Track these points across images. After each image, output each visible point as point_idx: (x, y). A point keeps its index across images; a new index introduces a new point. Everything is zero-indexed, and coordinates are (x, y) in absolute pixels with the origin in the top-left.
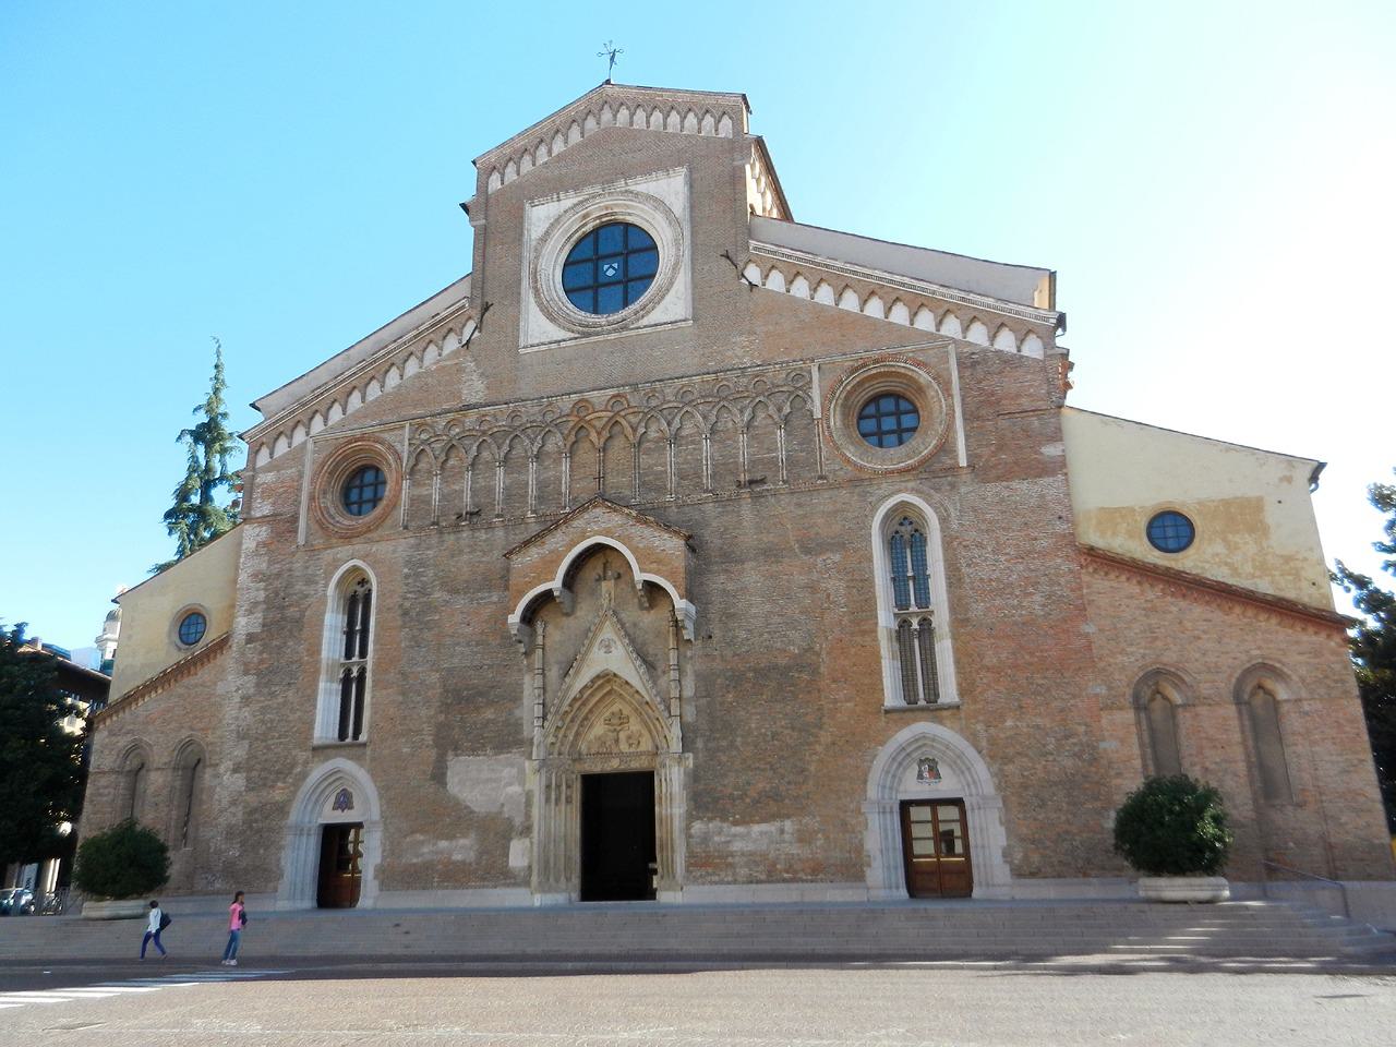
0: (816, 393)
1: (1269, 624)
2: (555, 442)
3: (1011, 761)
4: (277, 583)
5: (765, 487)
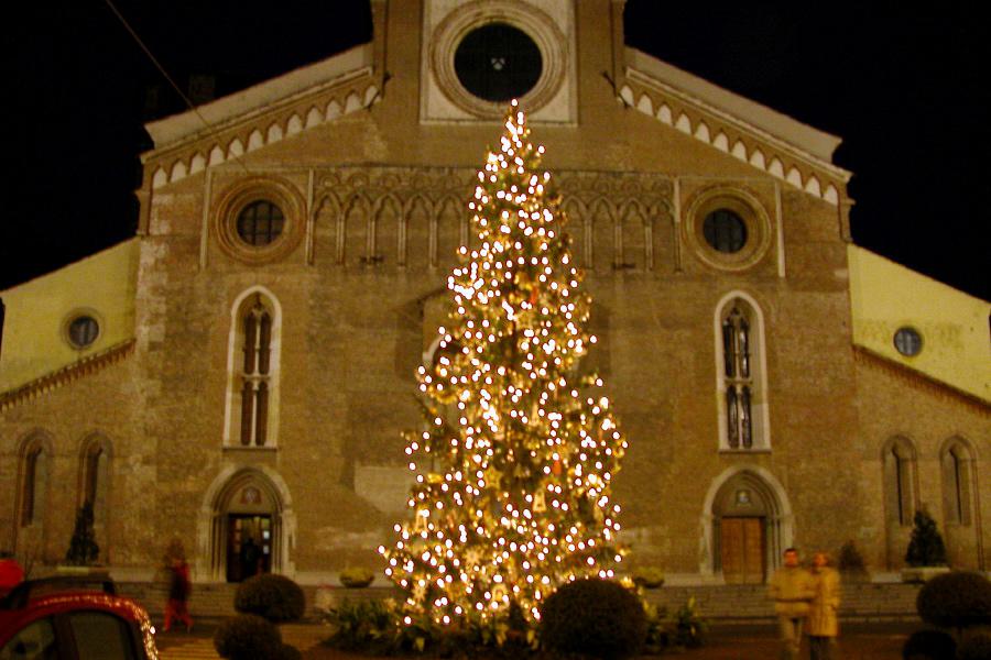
0: (677, 202)
1: (962, 409)
4: (179, 299)
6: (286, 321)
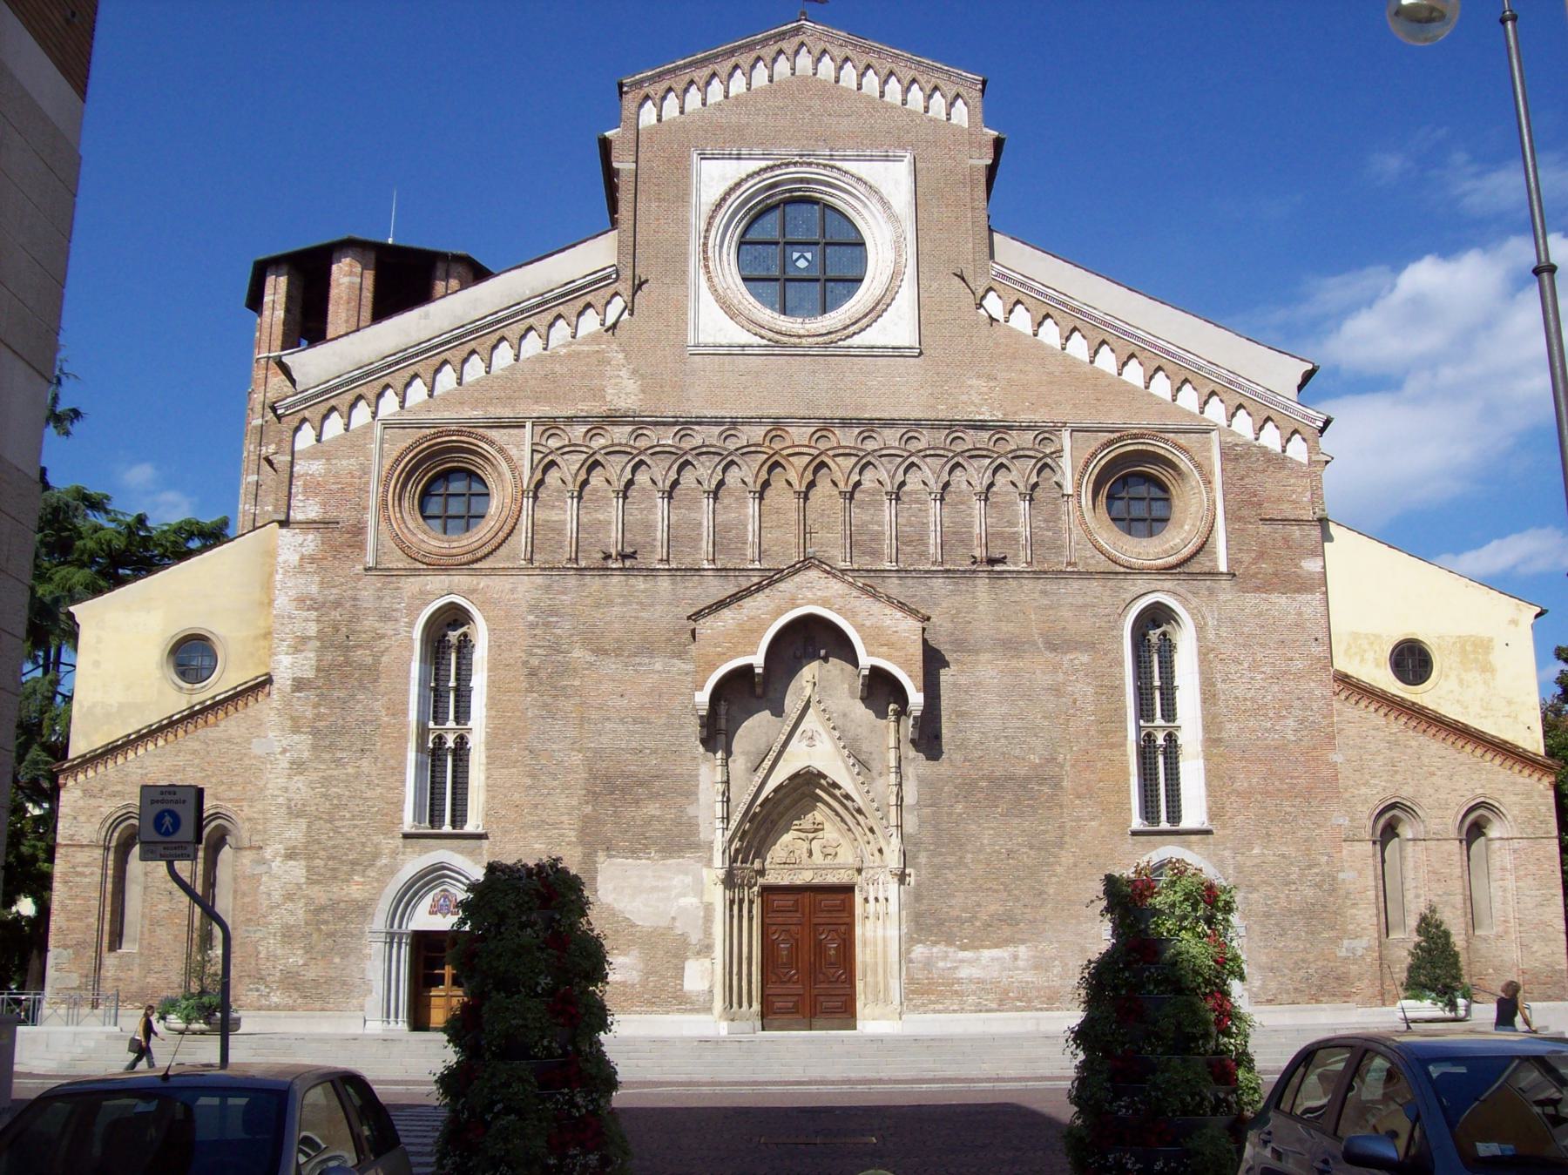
0: (1066, 463)
2: (746, 472)
3: (1256, 890)
4: (335, 614)
5: (1004, 568)
6: (495, 647)
